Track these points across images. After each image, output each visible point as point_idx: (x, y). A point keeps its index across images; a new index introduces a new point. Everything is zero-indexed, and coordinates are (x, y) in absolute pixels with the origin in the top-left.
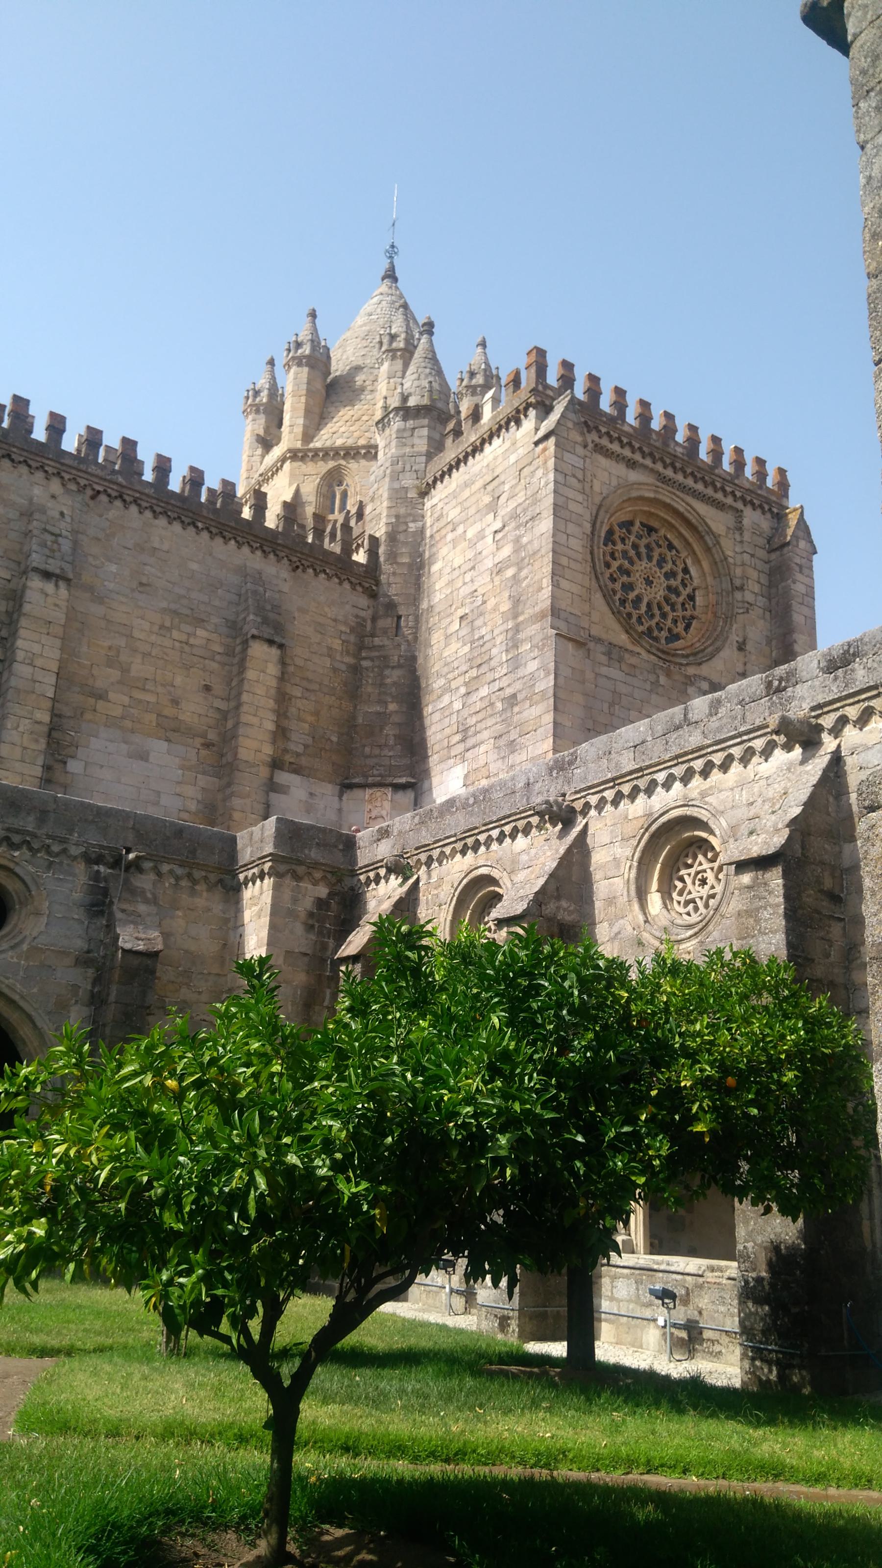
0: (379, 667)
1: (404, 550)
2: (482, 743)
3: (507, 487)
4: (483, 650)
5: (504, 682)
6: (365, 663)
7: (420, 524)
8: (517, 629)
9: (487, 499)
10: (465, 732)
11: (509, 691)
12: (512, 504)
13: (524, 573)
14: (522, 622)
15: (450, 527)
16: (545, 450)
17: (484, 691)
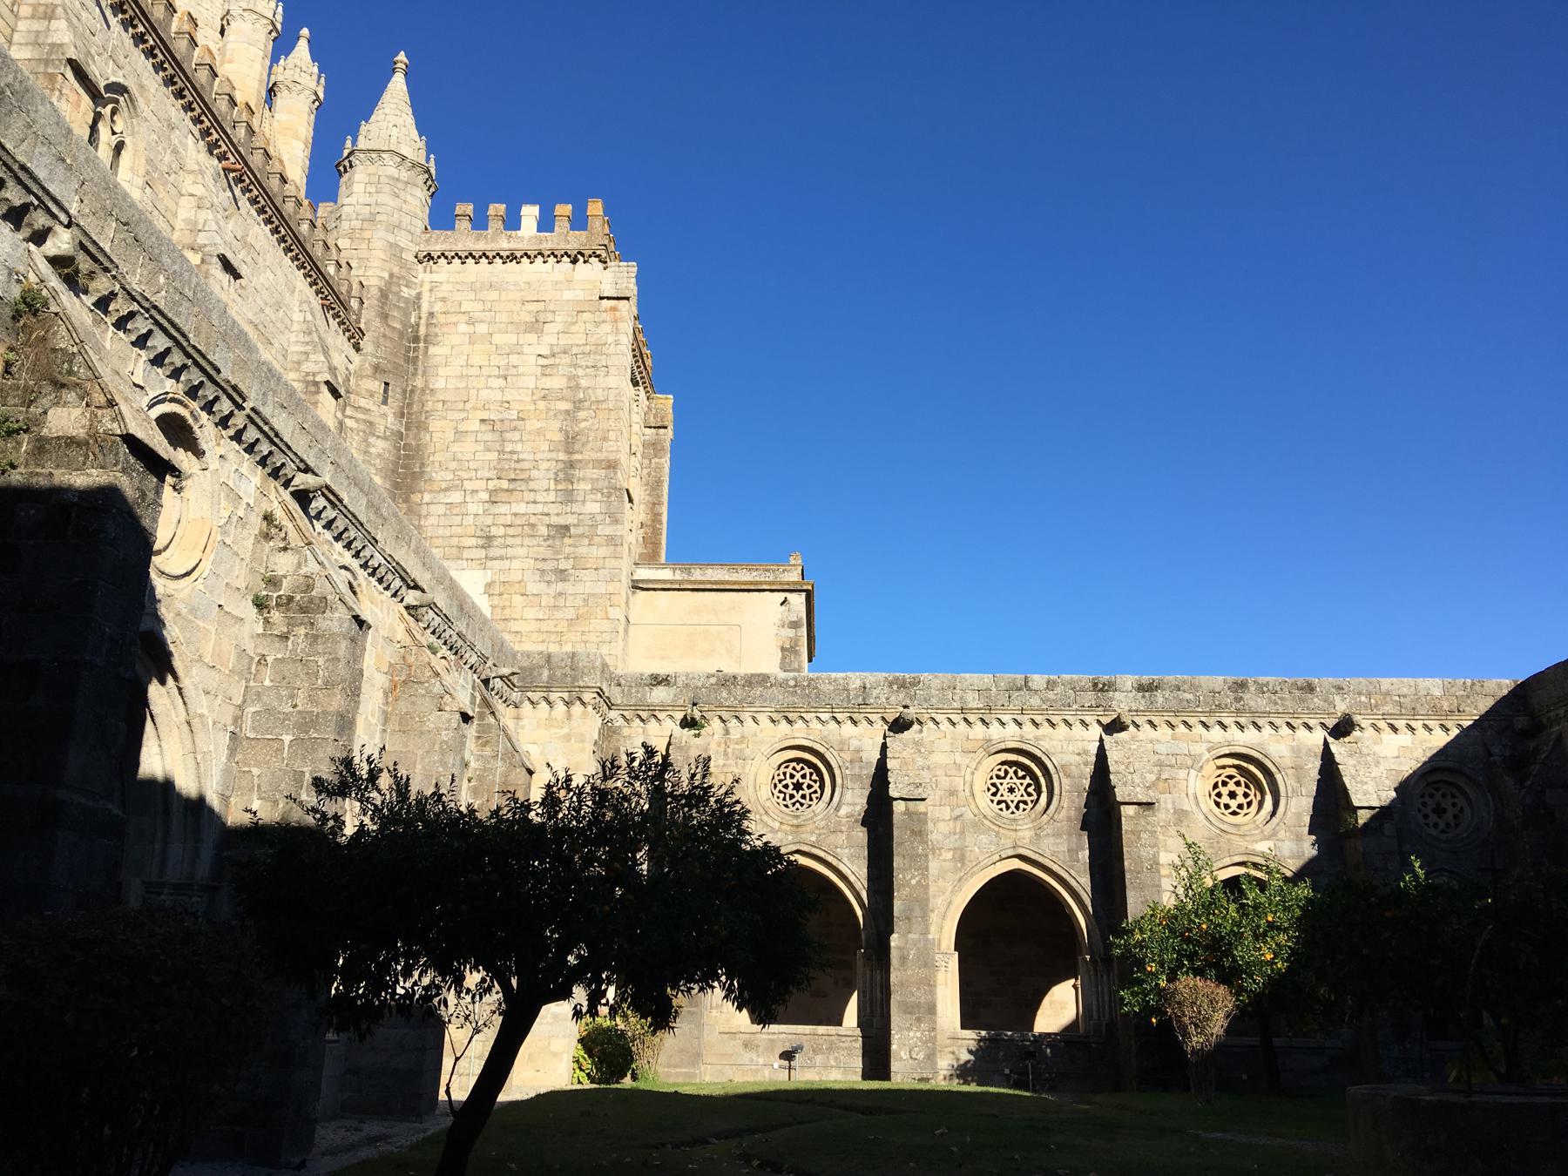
0: (364, 432)
1: (395, 314)
2: (515, 558)
3: (558, 319)
4: (518, 466)
5: (553, 509)
6: (349, 423)
7: (414, 293)
8: (571, 465)
9: (529, 318)
10: (488, 541)
11: (555, 520)
12: (565, 340)
13: (582, 415)
14: (580, 461)
15: (465, 318)
16: (614, 309)
17: (521, 508)
